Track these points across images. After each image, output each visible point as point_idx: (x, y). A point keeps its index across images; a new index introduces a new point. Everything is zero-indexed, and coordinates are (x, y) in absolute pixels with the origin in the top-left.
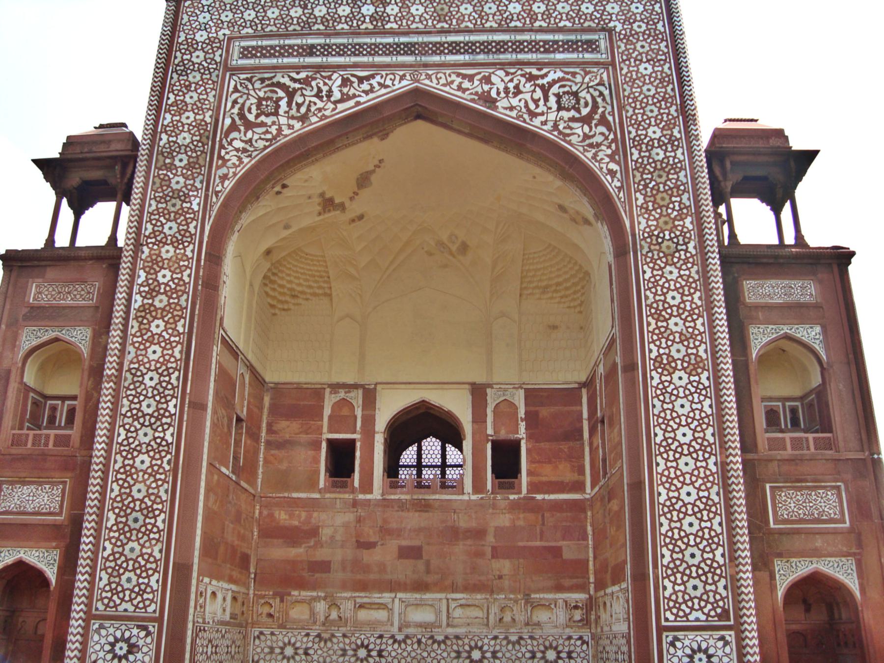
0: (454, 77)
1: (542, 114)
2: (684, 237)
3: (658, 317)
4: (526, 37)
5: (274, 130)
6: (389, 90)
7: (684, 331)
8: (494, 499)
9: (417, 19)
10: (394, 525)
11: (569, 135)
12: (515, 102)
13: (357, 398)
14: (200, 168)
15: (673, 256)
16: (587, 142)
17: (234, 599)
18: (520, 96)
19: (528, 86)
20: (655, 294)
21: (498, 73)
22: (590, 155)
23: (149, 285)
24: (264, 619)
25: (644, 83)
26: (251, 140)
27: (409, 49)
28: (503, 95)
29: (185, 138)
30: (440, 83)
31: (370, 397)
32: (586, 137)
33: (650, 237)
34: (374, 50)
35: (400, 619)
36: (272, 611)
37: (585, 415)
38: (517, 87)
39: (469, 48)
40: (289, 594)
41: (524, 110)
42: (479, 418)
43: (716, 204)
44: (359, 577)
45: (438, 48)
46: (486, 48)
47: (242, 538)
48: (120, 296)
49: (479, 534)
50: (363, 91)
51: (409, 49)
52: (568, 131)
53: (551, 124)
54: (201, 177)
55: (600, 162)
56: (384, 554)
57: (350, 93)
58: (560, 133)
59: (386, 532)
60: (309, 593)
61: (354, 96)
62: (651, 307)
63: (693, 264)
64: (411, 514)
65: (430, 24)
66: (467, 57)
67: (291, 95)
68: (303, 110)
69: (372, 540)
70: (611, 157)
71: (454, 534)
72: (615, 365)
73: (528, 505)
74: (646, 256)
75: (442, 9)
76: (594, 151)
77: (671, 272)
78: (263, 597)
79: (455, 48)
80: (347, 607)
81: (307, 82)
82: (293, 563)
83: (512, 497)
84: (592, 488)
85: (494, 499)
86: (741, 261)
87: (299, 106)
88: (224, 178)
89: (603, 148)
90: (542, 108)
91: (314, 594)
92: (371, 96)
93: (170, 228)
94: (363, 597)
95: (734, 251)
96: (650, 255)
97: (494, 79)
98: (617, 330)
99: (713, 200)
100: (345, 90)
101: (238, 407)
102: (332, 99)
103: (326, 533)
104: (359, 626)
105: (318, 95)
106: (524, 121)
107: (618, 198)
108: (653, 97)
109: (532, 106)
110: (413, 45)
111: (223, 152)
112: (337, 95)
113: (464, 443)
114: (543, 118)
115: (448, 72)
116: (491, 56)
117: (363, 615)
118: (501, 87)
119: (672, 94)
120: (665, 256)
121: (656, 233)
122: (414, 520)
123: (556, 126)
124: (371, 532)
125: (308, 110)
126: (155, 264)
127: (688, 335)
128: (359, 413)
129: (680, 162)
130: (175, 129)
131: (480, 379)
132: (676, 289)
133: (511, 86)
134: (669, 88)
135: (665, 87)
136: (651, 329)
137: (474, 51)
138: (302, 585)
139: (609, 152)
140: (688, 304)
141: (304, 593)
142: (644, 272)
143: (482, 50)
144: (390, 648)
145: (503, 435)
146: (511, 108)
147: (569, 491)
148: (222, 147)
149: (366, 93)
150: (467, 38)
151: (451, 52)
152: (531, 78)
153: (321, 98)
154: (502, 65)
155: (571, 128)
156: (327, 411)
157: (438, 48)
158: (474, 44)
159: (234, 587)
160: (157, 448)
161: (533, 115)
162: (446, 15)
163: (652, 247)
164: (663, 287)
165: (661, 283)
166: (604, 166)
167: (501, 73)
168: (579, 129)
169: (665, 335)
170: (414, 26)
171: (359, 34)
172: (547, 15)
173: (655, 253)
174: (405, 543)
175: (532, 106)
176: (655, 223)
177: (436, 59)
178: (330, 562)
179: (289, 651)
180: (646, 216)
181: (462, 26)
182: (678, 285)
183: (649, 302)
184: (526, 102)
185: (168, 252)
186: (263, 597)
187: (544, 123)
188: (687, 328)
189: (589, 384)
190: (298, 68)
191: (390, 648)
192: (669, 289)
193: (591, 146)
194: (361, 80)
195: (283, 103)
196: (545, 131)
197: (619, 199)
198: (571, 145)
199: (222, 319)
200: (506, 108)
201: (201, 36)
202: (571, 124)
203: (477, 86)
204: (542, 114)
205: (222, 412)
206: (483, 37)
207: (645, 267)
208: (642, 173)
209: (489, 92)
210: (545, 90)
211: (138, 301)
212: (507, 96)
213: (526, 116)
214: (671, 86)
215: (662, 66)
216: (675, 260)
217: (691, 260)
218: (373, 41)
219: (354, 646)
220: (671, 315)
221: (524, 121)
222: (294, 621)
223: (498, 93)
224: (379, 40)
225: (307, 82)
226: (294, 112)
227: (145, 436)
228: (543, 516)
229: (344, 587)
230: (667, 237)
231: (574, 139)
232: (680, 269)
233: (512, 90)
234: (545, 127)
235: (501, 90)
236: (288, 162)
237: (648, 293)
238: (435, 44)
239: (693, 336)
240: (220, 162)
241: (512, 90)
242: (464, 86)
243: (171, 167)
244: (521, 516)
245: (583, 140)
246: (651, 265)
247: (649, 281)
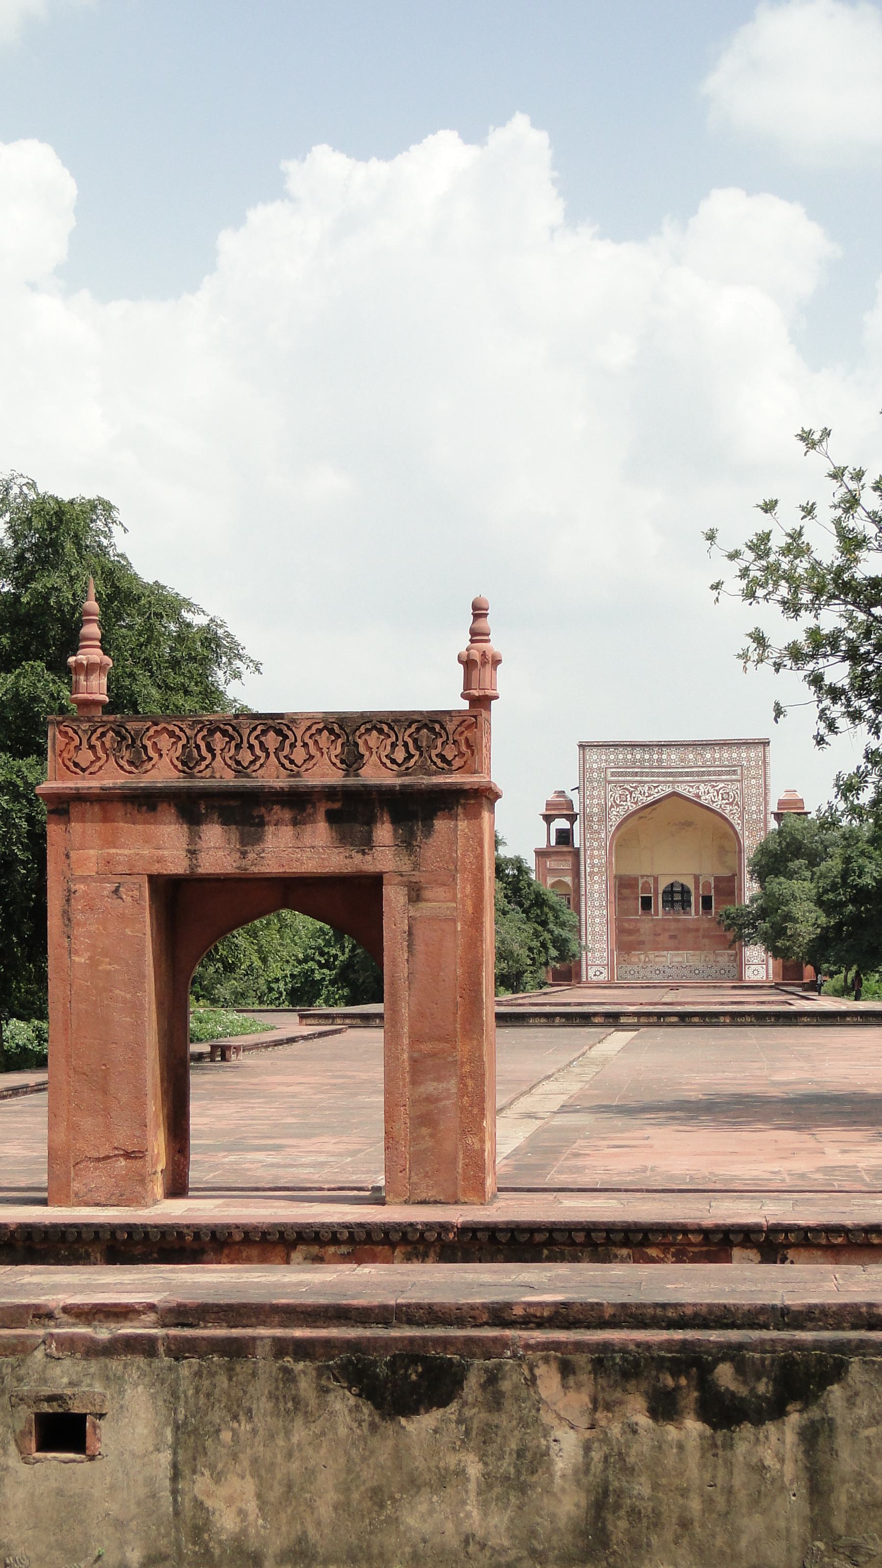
4: (712, 769)
12: (707, 797)
13: (651, 881)
19: (712, 791)
27: (671, 774)
29: (595, 810)
30: (681, 789)
31: (656, 880)
42: (697, 888)
45: (681, 774)
48: (582, 868)
49: (697, 930)
51: (671, 774)
56: (664, 938)
59: (665, 930)
67: (631, 793)
71: (688, 930)
80: (652, 957)
81: (636, 788)
88: (611, 826)
93: (595, 844)
94: (657, 953)
103: (642, 931)
104: (656, 963)
105: (640, 793)
107: (740, 832)
112: (647, 794)
117: (657, 959)
122: (673, 925)
126: (592, 857)
128: (652, 886)
130: (592, 806)
131: (697, 873)
138: (635, 950)
144: (667, 970)
145: (706, 894)
152: (713, 787)
156: (640, 886)
157: (681, 774)
160: (602, 916)
172: (720, 759)
179: (632, 972)
185: (596, 853)
190: (633, 782)
191: (667, 970)
194: (655, 787)
195: (628, 796)
201: (595, 766)
211: (588, 870)
225: (636, 788)
227: (597, 913)
229: (650, 950)
243: (592, 821)
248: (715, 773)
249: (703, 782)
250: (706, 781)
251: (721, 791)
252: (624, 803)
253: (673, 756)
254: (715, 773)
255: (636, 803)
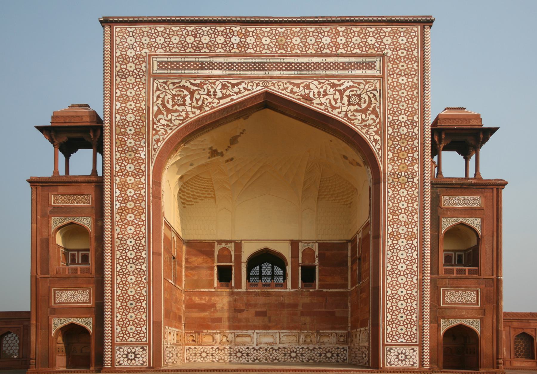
0: (288, 85)
1: (339, 107)
2: (413, 175)
3: (394, 213)
5: (184, 114)
6: (250, 92)
7: (407, 221)
8: (302, 291)
9: (266, 47)
10: (253, 302)
11: (353, 120)
12: (323, 100)
14: (143, 135)
15: (405, 184)
16: (364, 124)
17: (177, 334)
18: (327, 97)
20: (393, 203)
21: (314, 82)
22: (364, 131)
23: (122, 197)
24: (191, 342)
25: (401, 89)
26: (171, 120)
28: (316, 96)
32: (363, 120)
33: (394, 175)
34: (240, 66)
35: (257, 341)
36: (194, 339)
37: (349, 254)
38: (325, 91)
39: (298, 67)
40: (202, 332)
41: (328, 105)
43: (432, 157)
44: (236, 324)
46: (307, 66)
47: (178, 309)
49: (295, 306)
50: (235, 93)
52: (353, 118)
53: (343, 113)
54: (144, 140)
55: (369, 135)
57: (227, 93)
58: (349, 118)
59: (249, 305)
60: (212, 331)
61: (230, 95)
62: (390, 209)
63: (416, 188)
64: (261, 297)
65: (274, 50)
66: (296, 72)
68: (200, 103)
69: (242, 308)
70: (376, 133)
72: (368, 235)
73: (318, 294)
74: (390, 184)
75: (281, 40)
76: (367, 129)
77: (403, 192)
78: (190, 333)
79: (289, 66)
82: (203, 319)
83: (311, 290)
84: (352, 287)
85: (302, 291)
86: (442, 186)
87: (197, 100)
89: (372, 127)
90: (339, 104)
91: (215, 331)
92: (240, 95)
95: (440, 181)
96: (393, 184)
97: (312, 86)
98: (371, 219)
99: (431, 153)
100: (224, 91)
101: (173, 252)
102: (217, 97)
105: (208, 94)
106: (328, 112)
108: (405, 97)
109: (333, 103)
110: (264, 64)
111: (155, 126)
112: (219, 95)
113: (287, 267)
114: (339, 110)
115: (285, 82)
116: (310, 72)
118: (316, 91)
119: (416, 95)
120: (401, 184)
121: (397, 173)
122: (262, 300)
123: (346, 115)
124: (241, 305)
125: (203, 103)
127: (409, 223)
129: (416, 135)
132: (405, 201)
133: (321, 90)
134: (415, 92)
135: (412, 91)
136: (389, 219)
137: (300, 68)
138: (208, 328)
139: (375, 129)
140: (410, 208)
141: (209, 331)
142: (388, 192)
143: (305, 68)
146: (321, 104)
147: (339, 289)
148: (154, 123)
149: (237, 93)
150: (296, 60)
151: (286, 69)
153: (210, 96)
154: (317, 78)
155: (355, 116)
158: (300, 64)
159: (177, 330)
161: (333, 108)
162: (284, 45)
163: (394, 180)
164: (398, 199)
165: (397, 198)
166: (372, 137)
167: (316, 83)
168: (359, 116)
169: (397, 222)
170: (264, 51)
171: (231, 56)
173: (396, 183)
174: (258, 310)
175: (333, 103)
176: (397, 167)
177: (277, 73)
178: (221, 318)
180: (393, 164)
181: (294, 52)
182: (406, 199)
183: (390, 207)
184: (330, 100)
186: (190, 333)
187: (340, 113)
188: (408, 219)
189: (353, 241)
192: (401, 201)
193: (365, 126)
195: (188, 98)
196: (340, 118)
197: (379, 155)
198: (354, 125)
199: (163, 213)
200: (318, 104)
202: (355, 113)
203: (302, 91)
204: (339, 107)
205: (167, 255)
206: (306, 60)
207: (389, 190)
208: (393, 141)
209: (308, 94)
210: (341, 93)
212: (319, 97)
213: (329, 109)
214: (416, 91)
215: (412, 78)
216: (406, 186)
217: (415, 186)
218: (240, 61)
219: (235, 352)
220: (401, 213)
221: (328, 112)
222: (206, 343)
223: (314, 95)
224: (243, 60)
226: (194, 104)
228: (326, 299)
230: (403, 175)
231: (356, 122)
232: (408, 191)
233: (322, 93)
234: (340, 115)
235: (316, 93)
236: (193, 133)
237: (390, 202)
238: (277, 64)
239: (411, 223)
240: (154, 132)
241: (322, 93)
242: (294, 90)
244: (316, 298)
245: (362, 123)
246: (393, 189)
247: (391, 197)
248: (336, 66)
249: (317, 78)
250: (322, 77)
251: (347, 93)
252: (180, 108)
253: (267, 37)
254: (336, 66)
255: (201, 108)
